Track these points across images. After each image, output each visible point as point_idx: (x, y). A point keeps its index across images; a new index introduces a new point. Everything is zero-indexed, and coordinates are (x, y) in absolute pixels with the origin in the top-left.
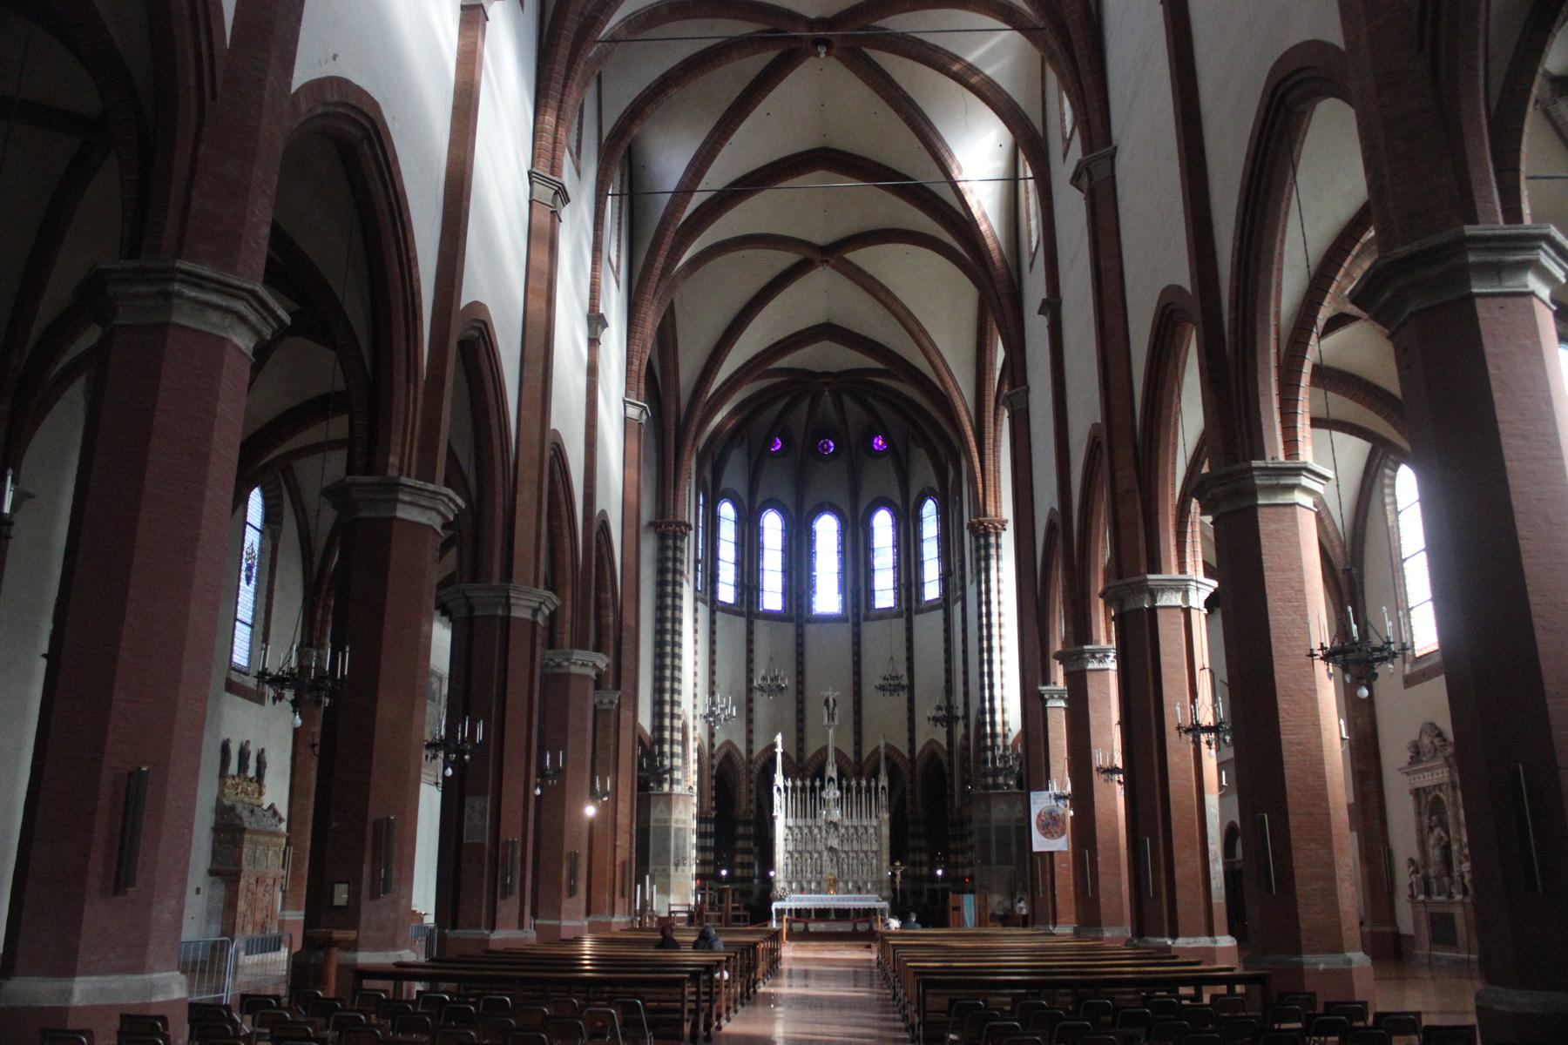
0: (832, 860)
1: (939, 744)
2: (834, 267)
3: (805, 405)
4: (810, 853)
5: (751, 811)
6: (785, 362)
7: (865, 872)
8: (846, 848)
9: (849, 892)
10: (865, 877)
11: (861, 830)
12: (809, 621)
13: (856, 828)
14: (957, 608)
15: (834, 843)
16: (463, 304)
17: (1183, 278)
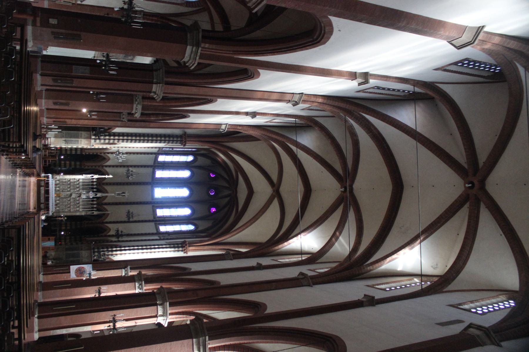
0: (67, 195)
1: (109, 232)
2: (272, 194)
3: (227, 185)
4: (70, 188)
5: (85, 167)
6: (241, 179)
7: (63, 207)
8: (72, 200)
9: (55, 201)
10: (61, 207)
11: (78, 205)
13: (79, 203)
14: (157, 238)
15: (74, 196)
16: (260, 70)
17: (269, 311)
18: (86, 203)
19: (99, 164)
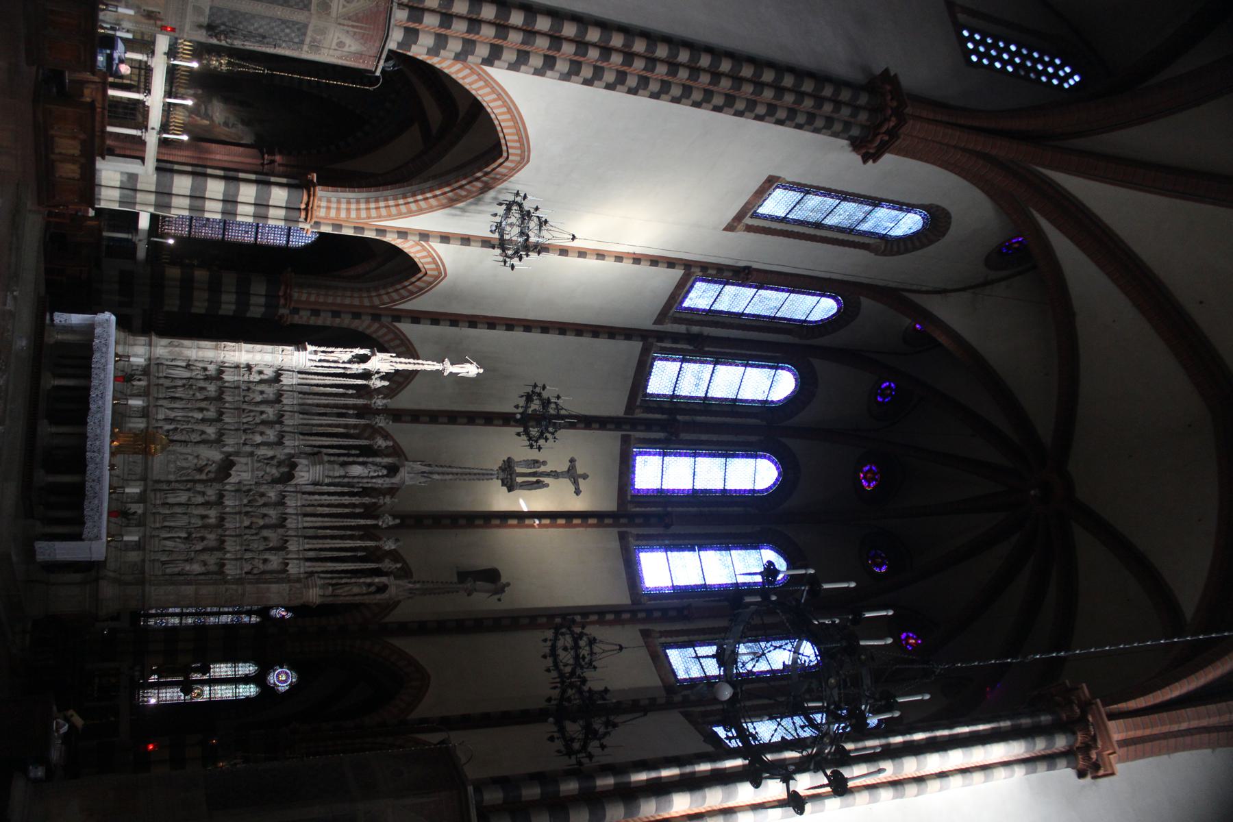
12: (622, 537)
15: (242, 474)
18: (328, 522)
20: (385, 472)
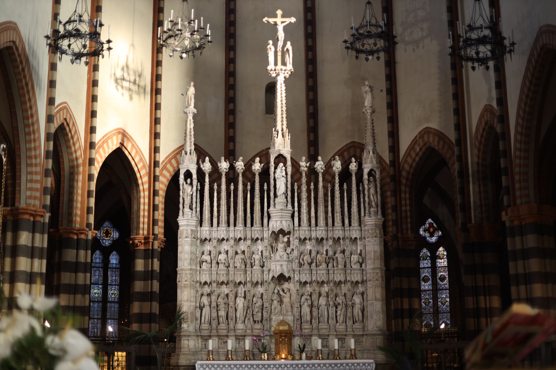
5: (156, 237)
7: (341, 319)
10: (341, 327)
18: (321, 209)
19: (146, 179)
20: (281, 165)
